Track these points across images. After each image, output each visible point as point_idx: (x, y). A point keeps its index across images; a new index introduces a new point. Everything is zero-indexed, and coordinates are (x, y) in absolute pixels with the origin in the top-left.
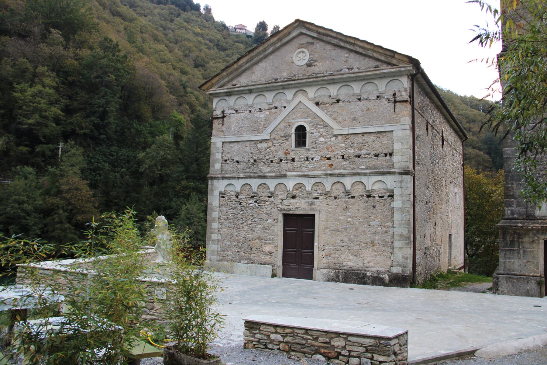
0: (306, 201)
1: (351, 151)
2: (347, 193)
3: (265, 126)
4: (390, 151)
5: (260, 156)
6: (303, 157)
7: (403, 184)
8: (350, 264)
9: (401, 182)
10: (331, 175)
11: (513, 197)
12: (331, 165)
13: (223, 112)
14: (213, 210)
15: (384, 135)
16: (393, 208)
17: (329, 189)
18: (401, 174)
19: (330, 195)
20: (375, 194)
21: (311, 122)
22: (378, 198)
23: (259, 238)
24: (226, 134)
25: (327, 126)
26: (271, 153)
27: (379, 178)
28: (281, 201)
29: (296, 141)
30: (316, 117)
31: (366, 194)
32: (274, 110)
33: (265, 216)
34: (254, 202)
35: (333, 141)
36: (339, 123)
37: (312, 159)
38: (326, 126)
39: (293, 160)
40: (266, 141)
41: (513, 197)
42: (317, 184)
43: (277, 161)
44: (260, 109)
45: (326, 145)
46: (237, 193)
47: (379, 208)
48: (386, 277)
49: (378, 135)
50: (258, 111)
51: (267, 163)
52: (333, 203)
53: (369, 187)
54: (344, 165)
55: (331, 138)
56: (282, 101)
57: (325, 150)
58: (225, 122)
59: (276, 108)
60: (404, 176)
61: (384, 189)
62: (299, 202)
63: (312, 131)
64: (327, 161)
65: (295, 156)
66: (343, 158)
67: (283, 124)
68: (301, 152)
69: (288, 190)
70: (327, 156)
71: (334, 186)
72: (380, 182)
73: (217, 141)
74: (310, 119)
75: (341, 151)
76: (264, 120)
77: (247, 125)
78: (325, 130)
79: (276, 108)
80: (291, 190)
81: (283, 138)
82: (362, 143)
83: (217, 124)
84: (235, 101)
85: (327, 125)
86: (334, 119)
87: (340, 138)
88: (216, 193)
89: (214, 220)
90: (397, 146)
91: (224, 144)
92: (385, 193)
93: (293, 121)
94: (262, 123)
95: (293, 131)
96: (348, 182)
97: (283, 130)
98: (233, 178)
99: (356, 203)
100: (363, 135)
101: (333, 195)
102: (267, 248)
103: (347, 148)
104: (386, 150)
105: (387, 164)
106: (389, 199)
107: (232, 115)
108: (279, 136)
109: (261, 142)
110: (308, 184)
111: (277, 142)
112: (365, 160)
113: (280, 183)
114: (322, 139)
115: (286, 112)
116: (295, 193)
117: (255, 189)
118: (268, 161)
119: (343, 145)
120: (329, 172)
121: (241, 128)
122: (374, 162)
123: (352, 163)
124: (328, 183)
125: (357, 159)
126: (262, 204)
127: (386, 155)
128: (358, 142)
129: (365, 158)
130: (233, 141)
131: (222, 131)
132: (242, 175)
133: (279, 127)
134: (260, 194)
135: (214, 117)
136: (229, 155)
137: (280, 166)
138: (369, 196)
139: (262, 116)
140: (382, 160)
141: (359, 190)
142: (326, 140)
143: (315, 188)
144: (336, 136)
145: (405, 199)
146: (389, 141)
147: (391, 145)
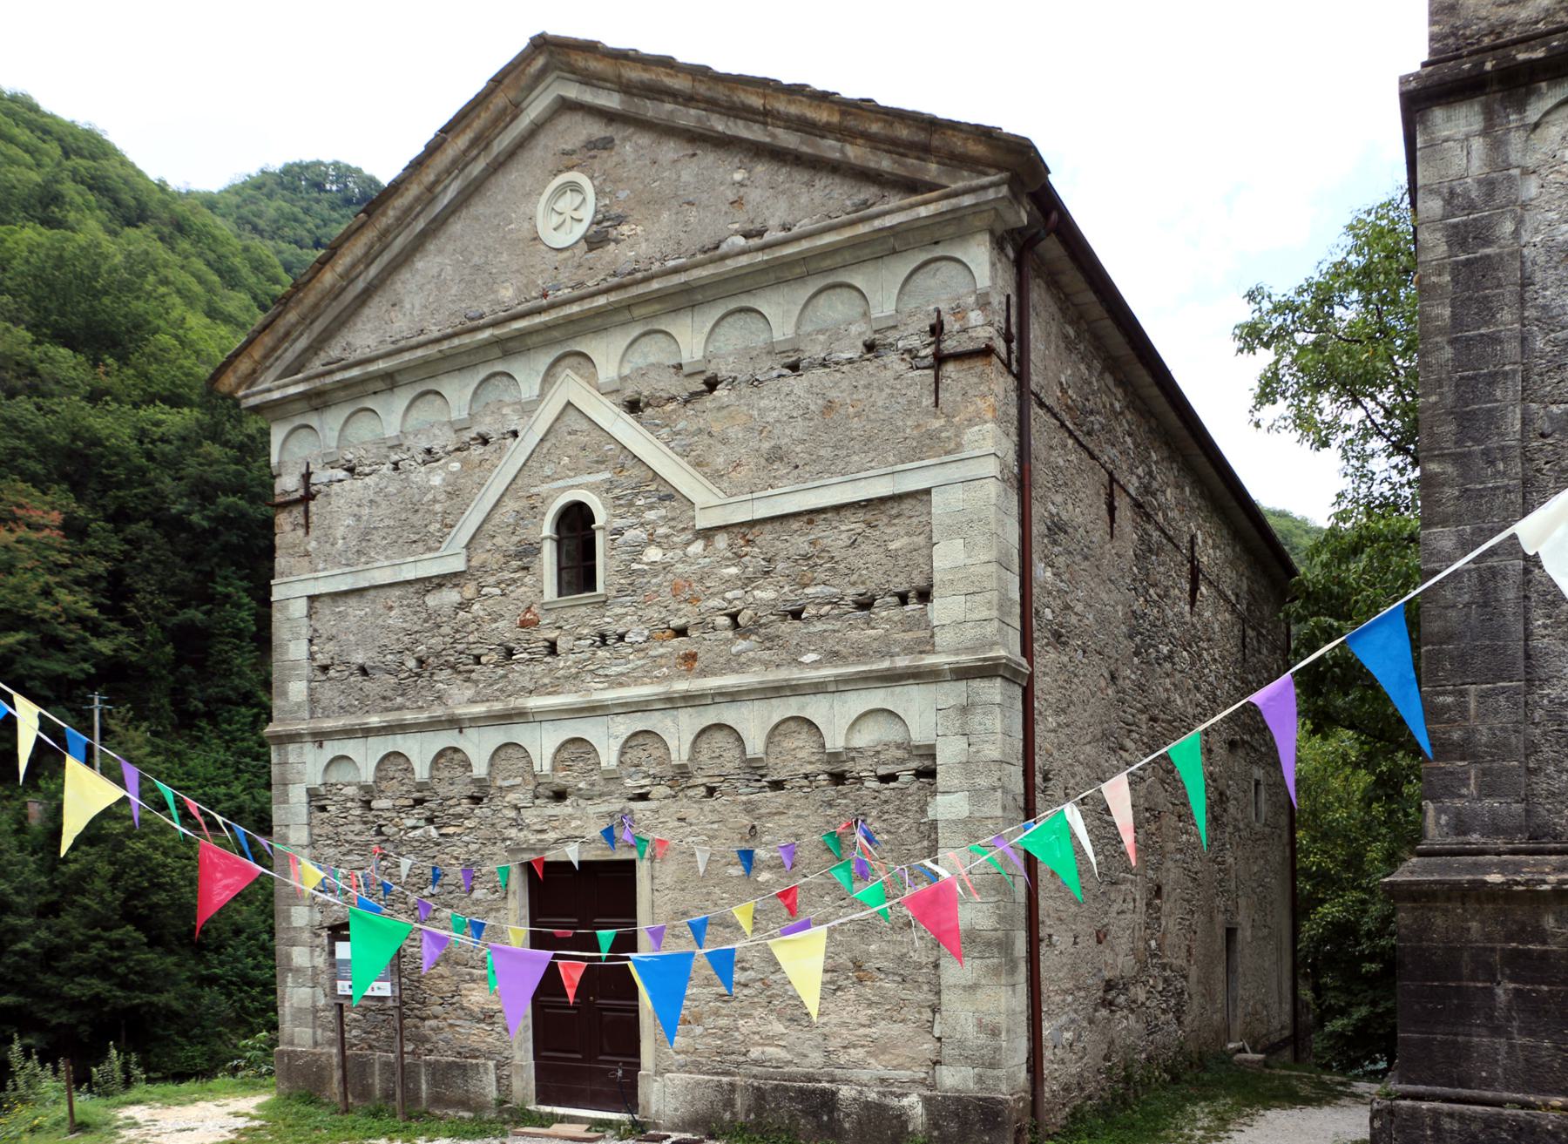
0: (604, 808)
1: (766, 594)
2: (754, 769)
3: (448, 521)
4: (919, 581)
6: (585, 632)
7: (976, 720)
9: (965, 710)
10: (690, 700)
11: (1466, 750)
12: (690, 658)
13: (307, 476)
15: (894, 512)
16: (934, 825)
17: (684, 758)
18: (963, 674)
19: (691, 782)
20: (861, 767)
21: (611, 485)
22: (875, 784)
24: (321, 566)
25: (670, 497)
26: (473, 627)
27: (877, 698)
28: (513, 814)
29: (560, 570)
30: (629, 463)
31: (828, 768)
32: (477, 451)
34: (422, 823)
35: (697, 556)
36: (716, 477)
37: (621, 638)
38: (670, 495)
39: (552, 649)
40: (455, 581)
41: (1466, 750)
42: (640, 740)
43: (495, 657)
44: (429, 451)
45: (670, 576)
46: (365, 789)
47: (877, 825)
49: (869, 517)
50: (425, 463)
51: (462, 668)
52: (700, 812)
53: (835, 741)
54: (739, 654)
55: (688, 543)
56: (505, 411)
57: (666, 596)
58: (314, 518)
59: (485, 441)
60: (978, 684)
61: (898, 746)
62: (578, 814)
63: (618, 523)
64: (676, 641)
65: (557, 632)
66: (735, 625)
67: (511, 505)
68: (580, 614)
69: (537, 768)
70: (676, 622)
71: (703, 745)
72: (881, 718)
74: (607, 475)
75: (729, 595)
76: (442, 497)
77: (387, 522)
78: (663, 512)
79: (485, 441)
80: (547, 767)
81: (515, 564)
82: (806, 557)
83: (288, 528)
84: (342, 430)
85: (672, 491)
86: (698, 464)
87: (721, 541)
91: (317, 604)
92: (902, 761)
93: (544, 489)
94: (438, 507)
95: (547, 528)
96: (753, 723)
97: (510, 529)
98: (348, 733)
99: (789, 807)
100: (810, 522)
101: (700, 781)
103: (747, 582)
104: (902, 578)
105: (908, 636)
106: (917, 785)
107: (336, 487)
108: (498, 556)
109: (440, 586)
110: (607, 740)
111: (492, 580)
112: (819, 626)
113: (507, 745)
114: (653, 554)
115: (517, 453)
116: (561, 779)
117: (421, 772)
118: (463, 658)
119: (733, 570)
120: (681, 686)
121: (365, 536)
122: (853, 635)
123: (768, 644)
124: (678, 732)
125: (787, 627)
126: (450, 830)
127: (903, 599)
128: (792, 551)
129: (819, 617)
130: (344, 588)
131: (307, 554)
132: (374, 720)
133: (497, 518)
134: (443, 790)
135: (278, 500)
136: (331, 647)
137: (505, 676)
138: (838, 778)
139: (436, 480)
140: (889, 620)
141: (799, 755)
142: (670, 554)
143: (632, 755)
144: (707, 534)
145: (982, 782)
146: (915, 539)
147: (925, 552)
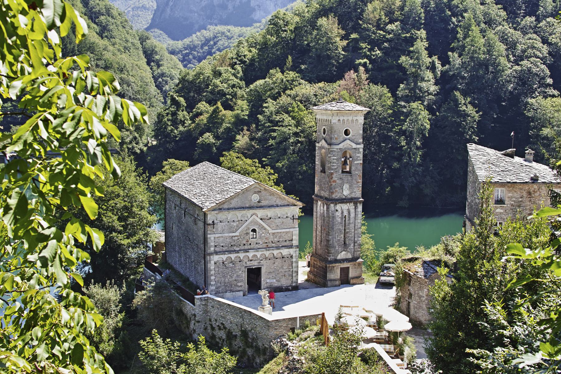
5: (234, 243)
8: (276, 285)
14: (211, 270)
23: (235, 280)
33: (238, 270)
38: (265, 229)
39: (250, 244)
48: (290, 288)
73: (211, 237)
88: (213, 262)
89: (212, 275)
90: (294, 238)
102: (239, 284)
114: (263, 235)
121: (224, 230)
138: (283, 257)
